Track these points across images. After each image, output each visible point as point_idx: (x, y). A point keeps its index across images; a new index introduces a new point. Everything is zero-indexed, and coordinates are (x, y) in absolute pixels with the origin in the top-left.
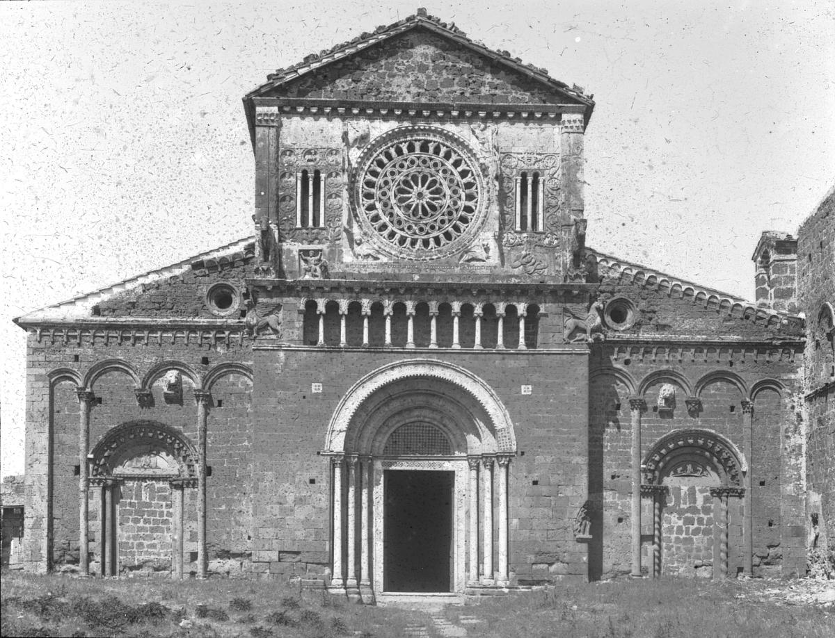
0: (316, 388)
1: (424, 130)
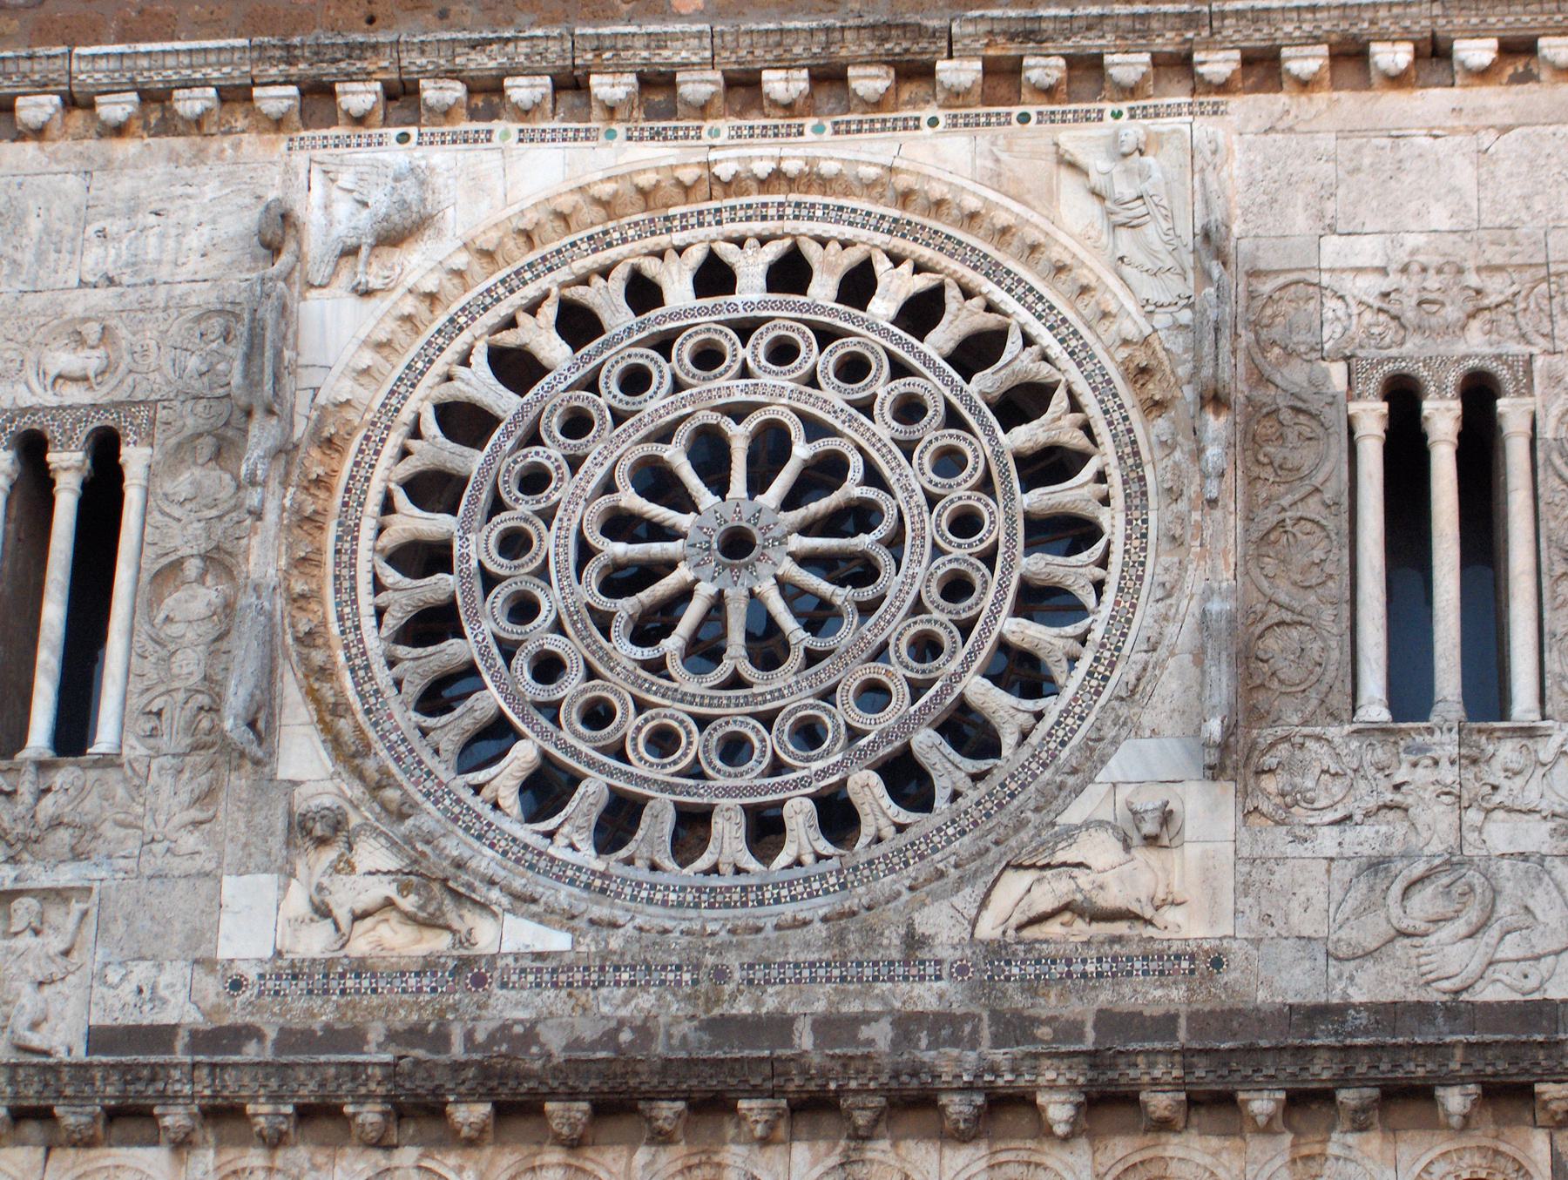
1: (776, 180)
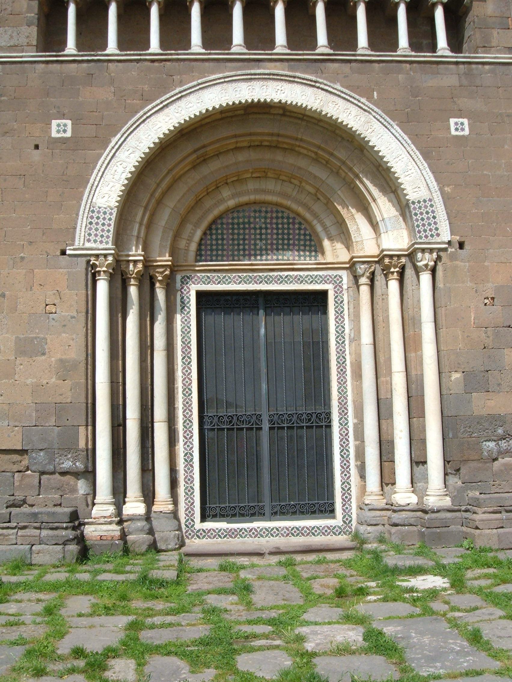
0: (61, 128)
